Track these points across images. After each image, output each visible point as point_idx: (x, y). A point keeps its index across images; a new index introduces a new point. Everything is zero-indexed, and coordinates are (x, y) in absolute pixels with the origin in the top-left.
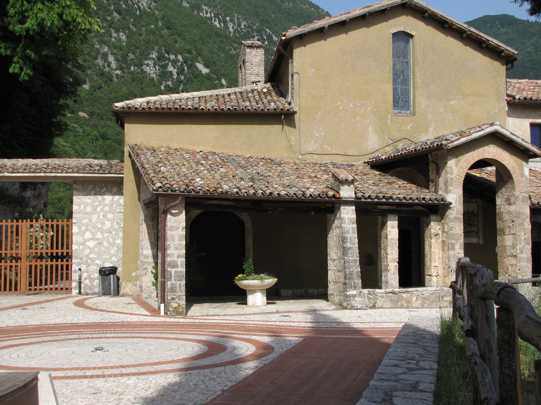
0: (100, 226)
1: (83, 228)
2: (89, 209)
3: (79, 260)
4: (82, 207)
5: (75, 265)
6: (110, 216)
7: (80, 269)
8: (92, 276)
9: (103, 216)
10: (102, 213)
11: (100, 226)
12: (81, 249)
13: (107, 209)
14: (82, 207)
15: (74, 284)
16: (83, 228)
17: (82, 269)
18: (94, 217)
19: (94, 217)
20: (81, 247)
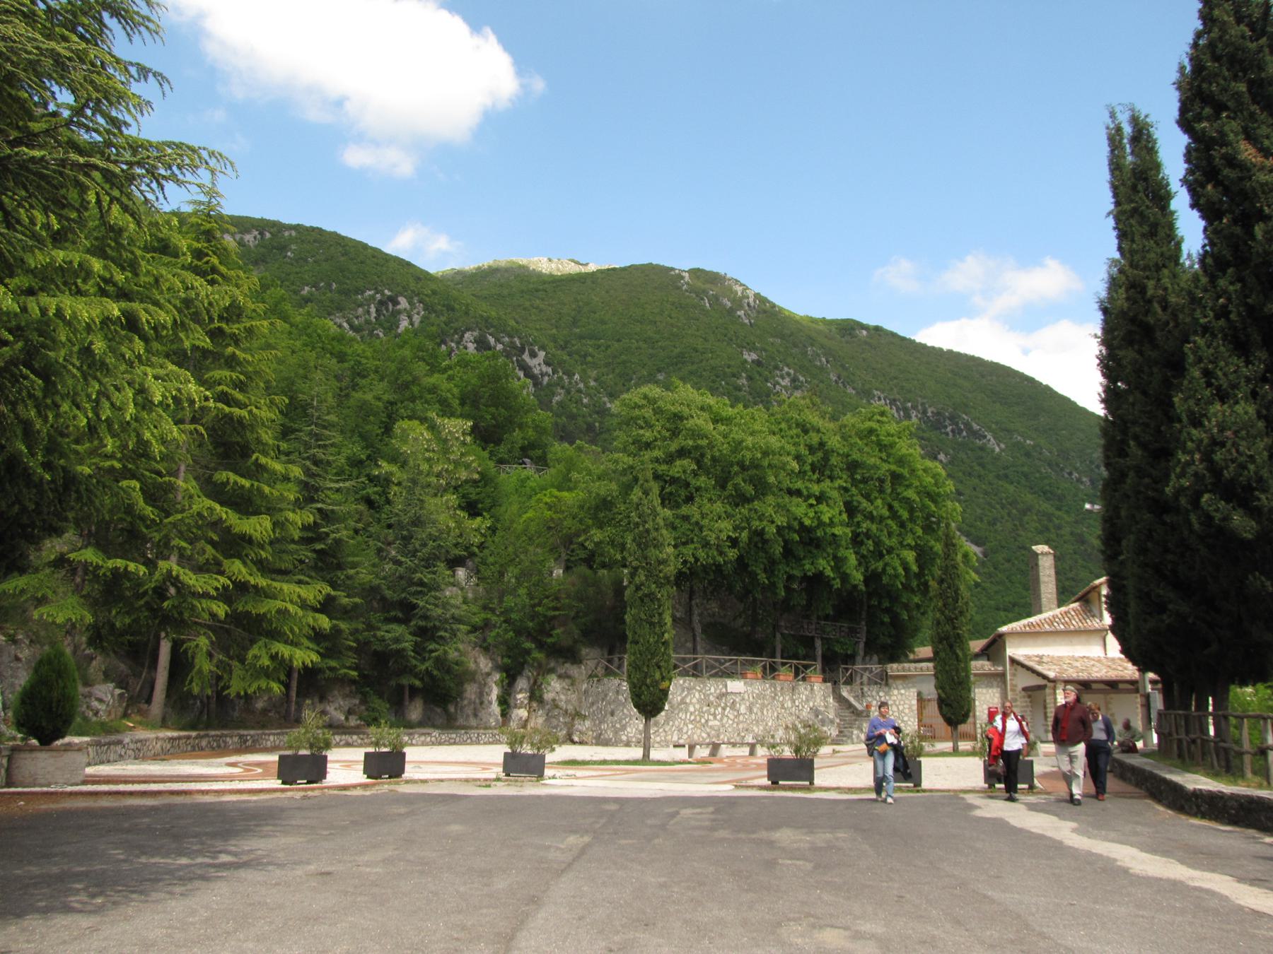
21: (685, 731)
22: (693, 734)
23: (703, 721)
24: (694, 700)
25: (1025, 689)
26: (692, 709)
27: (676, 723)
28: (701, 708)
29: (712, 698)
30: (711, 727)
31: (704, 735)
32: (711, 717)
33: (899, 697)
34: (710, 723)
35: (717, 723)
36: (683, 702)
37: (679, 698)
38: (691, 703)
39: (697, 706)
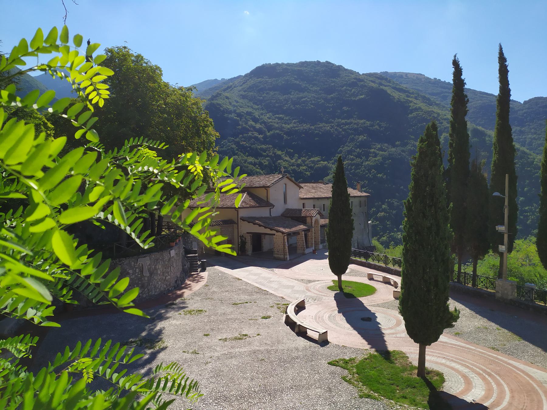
21: (157, 286)
22: (161, 287)
23: (164, 278)
24: (160, 267)
25: (247, 233)
26: (159, 272)
27: (153, 283)
28: (163, 270)
29: (166, 263)
30: (167, 281)
31: (165, 286)
32: (167, 274)
33: (193, 239)
34: (167, 278)
35: (169, 277)
36: (155, 269)
37: (153, 267)
38: (159, 268)
39: (161, 270)
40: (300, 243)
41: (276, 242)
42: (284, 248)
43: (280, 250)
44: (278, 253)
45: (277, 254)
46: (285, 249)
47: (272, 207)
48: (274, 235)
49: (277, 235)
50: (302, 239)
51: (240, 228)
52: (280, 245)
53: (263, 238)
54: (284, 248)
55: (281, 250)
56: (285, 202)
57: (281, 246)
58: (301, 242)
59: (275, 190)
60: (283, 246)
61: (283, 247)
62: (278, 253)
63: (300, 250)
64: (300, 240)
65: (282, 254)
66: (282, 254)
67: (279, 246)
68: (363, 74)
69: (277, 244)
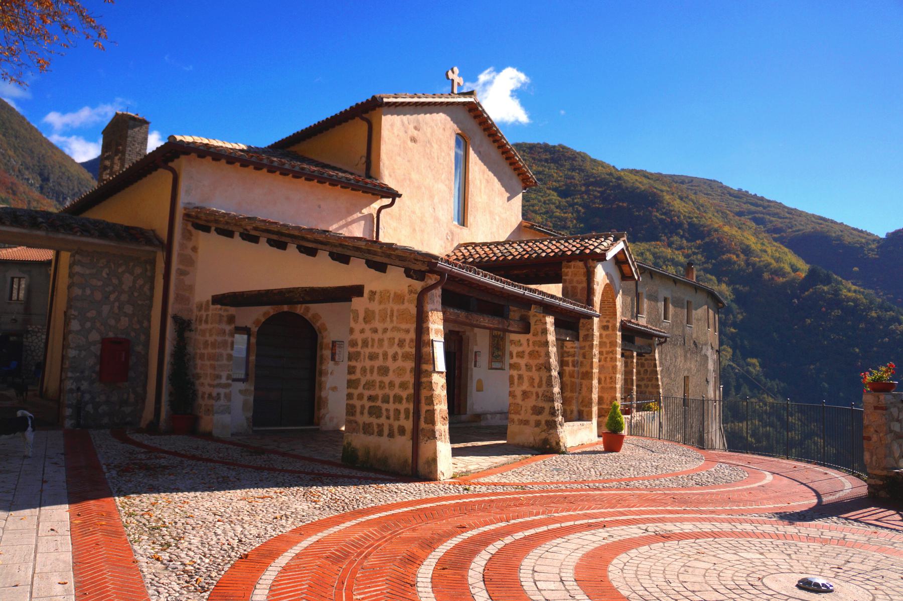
0: (112, 322)
1: (88, 325)
2: (98, 296)
3: (78, 374)
4: (88, 292)
5: (72, 381)
6: (129, 309)
7: (78, 389)
8: (97, 400)
9: (119, 307)
10: (117, 304)
11: (112, 322)
12: (82, 356)
13: (124, 297)
14: (88, 292)
15: (68, 412)
16: (88, 325)
17: (83, 388)
18: (106, 309)
19: (106, 309)
20: (84, 353)
40: (532, 384)
41: (365, 343)
42: (418, 385)
43: (386, 400)
44: (374, 421)
45: (367, 429)
46: (424, 393)
47: (387, 201)
48: (357, 291)
49: (373, 293)
50: (542, 360)
51: (181, 273)
52: (390, 363)
53: (327, 353)
54: (418, 385)
55: (398, 399)
56: (463, 221)
57: (400, 371)
58: (536, 375)
59: (414, 140)
60: (410, 365)
61: (409, 378)
62: (374, 421)
63: (526, 422)
64: (528, 367)
65: (402, 431)
66: (402, 431)
67: (384, 371)
68: (623, 170)
69: (373, 357)
